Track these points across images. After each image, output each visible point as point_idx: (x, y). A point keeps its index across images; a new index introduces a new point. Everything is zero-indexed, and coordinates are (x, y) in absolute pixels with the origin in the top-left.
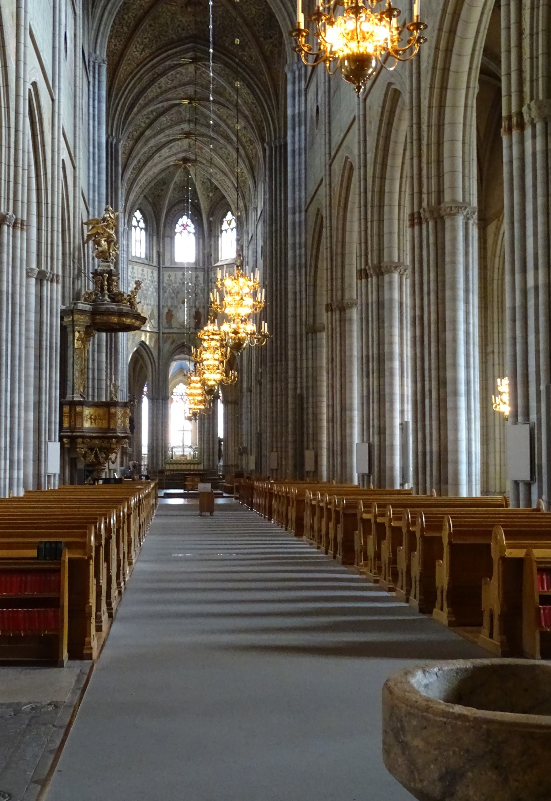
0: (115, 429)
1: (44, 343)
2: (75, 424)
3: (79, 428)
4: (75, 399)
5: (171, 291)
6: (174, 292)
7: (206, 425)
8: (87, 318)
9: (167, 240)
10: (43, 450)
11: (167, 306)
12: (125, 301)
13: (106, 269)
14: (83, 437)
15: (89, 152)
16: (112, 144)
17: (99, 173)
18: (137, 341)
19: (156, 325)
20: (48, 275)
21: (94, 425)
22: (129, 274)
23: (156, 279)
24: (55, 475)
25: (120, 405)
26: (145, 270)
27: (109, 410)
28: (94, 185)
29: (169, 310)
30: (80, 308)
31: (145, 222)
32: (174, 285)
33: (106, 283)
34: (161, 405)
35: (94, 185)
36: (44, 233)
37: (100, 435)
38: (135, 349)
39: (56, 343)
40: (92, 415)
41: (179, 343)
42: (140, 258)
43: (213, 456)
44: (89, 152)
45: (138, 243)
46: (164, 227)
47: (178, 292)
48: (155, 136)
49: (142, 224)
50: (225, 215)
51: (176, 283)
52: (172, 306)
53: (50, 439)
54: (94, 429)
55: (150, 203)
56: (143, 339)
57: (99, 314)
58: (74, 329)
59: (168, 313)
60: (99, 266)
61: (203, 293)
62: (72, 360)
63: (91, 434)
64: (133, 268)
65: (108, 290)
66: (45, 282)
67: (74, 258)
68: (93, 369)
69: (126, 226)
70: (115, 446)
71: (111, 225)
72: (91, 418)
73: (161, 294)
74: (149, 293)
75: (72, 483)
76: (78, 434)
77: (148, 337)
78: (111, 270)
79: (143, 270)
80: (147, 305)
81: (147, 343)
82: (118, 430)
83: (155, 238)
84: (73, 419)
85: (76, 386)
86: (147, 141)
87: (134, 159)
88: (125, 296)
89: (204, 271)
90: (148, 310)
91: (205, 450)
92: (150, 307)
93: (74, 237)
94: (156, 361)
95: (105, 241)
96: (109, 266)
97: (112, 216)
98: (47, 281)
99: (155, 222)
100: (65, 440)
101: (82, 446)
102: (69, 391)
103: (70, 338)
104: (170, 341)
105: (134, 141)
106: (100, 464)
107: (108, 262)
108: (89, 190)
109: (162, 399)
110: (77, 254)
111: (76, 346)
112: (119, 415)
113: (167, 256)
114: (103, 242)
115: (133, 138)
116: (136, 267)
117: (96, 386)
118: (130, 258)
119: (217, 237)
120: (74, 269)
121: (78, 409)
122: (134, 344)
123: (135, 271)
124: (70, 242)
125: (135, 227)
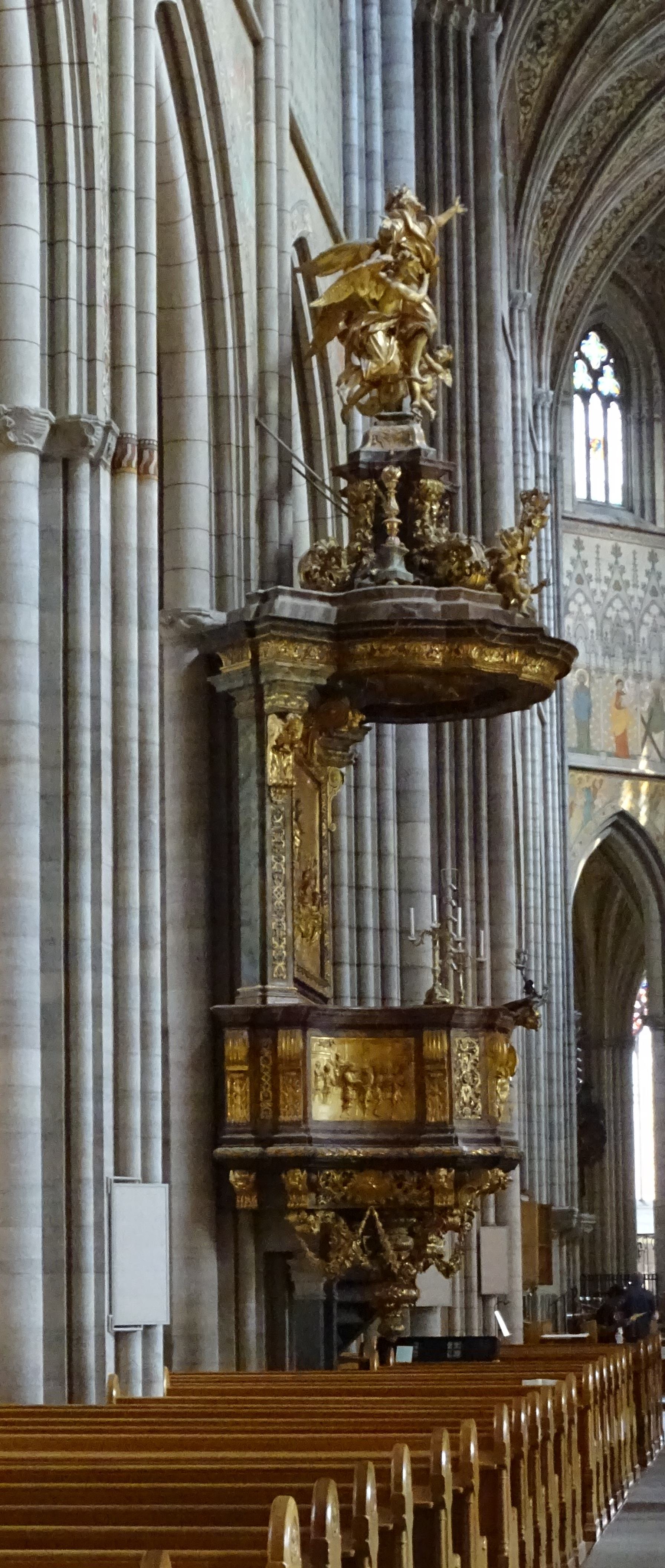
0: (444, 1127)
1: (86, 740)
2: (276, 1111)
3: (296, 1125)
4: (270, 1001)
8: (315, 653)
10: (89, 1218)
12: (477, 578)
13: (393, 447)
14: (309, 1163)
15: (344, 24)
16: (460, 35)
17: (387, 105)
18: (603, 815)
20: (95, 439)
21: (355, 1112)
22: (566, 566)
24: (148, 1329)
25: (468, 1020)
26: (626, 549)
27: (419, 1047)
28: (368, 155)
30: (286, 614)
31: (621, 373)
33: (394, 504)
35: (368, 155)
36: (74, 256)
37: (384, 1151)
38: (598, 841)
39: (143, 743)
40: (347, 1068)
42: (605, 506)
44: (344, 24)
45: (597, 456)
48: (640, 28)
49: (610, 384)
53: (121, 1168)
54: (358, 1126)
55: (639, 304)
56: (626, 804)
57: (365, 636)
58: (260, 700)
60: (366, 439)
62: (255, 833)
63: (345, 1151)
64: (579, 545)
65: (405, 533)
66: (85, 470)
67: (263, 412)
68: (382, 891)
69: (546, 384)
70: (450, 1200)
71: (414, 266)
72: (343, 1081)
74: (644, 633)
75: (274, 1362)
76: (288, 1149)
77: (643, 798)
78: (418, 451)
79: (616, 552)
80: (638, 676)
81: (643, 820)
82: (461, 1130)
84: (266, 1090)
85: (278, 947)
86: (612, 50)
87: (564, 121)
88: (478, 553)
90: (639, 697)
92: (647, 686)
93: (262, 330)
95: (390, 332)
96: (408, 437)
97: (419, 229)
98: (95, 465)
100: (234, 1176)
101: (308, 1201)
102: (248, 969)
103: (247, 742)
105: (559, 55)
106: (388, 1277)
107: (402, 419)
108: (346, 174)
110: (273, 396)
111: (273, 776)
112: (465, 1063)
114: (380, 337)
115: (555, 45)
116: (590, 542)
117: (395, 959)
118: (568, 508)
120: (263, 458)
121: (288, 1043)
122: (591, 825)
123: (588, 554)
124: (241, 347)
125: (585, 395)
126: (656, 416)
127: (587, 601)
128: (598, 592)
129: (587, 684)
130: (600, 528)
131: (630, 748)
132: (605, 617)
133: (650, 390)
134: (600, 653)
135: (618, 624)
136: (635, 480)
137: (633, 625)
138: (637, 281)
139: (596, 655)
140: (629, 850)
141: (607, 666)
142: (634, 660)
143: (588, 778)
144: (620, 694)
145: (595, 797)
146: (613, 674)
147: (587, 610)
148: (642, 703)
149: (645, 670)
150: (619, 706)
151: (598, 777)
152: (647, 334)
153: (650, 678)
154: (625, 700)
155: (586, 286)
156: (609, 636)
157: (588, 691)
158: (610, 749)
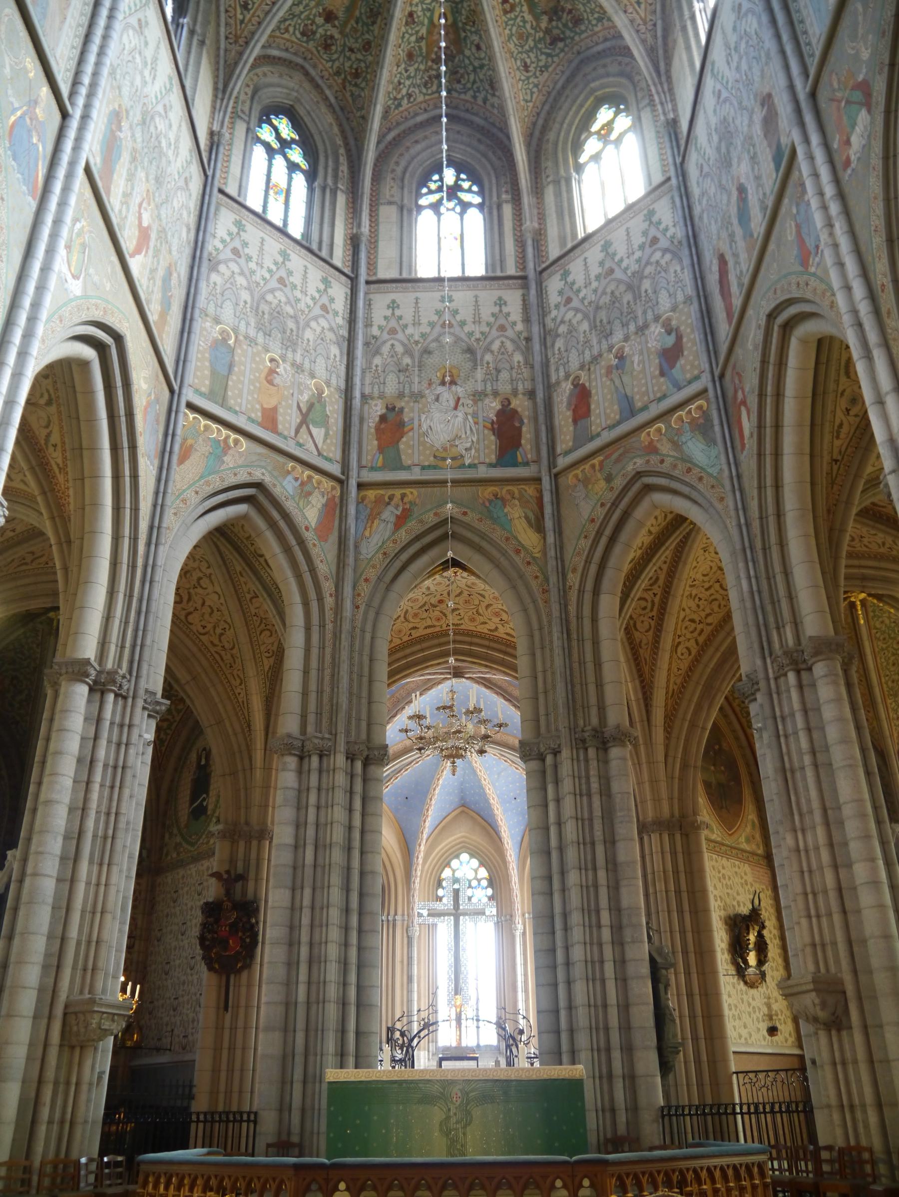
5: (399, 349)
6: (408, 352)
7: (573, 878)
9: (388, 213)
11: (382, 396)
19: (336, 453)
23: (340, 303)
29: (391, 409)
31: (310, 153)
32: (409, 331)
34: (341, 779)
41: (431, 519)
43: (628, 1049)
46: (377, 178)
47: (427, 352)
49: (296, 155)
50: (591, 116)
51: (417, 323)
52: (401, 395)
59: (383, 418)
61: (527, 351)
73: (359, 363)
74: (308, 334)
80: (298, 368)
83: (341, 199)
89: (526, 287)
91: (582, 1017)
94: (328, 587)
99: (343, 160)
104: (389, 514)
109: (351, 757)
113: (387, 252)
119: (563, 185)
126: (340, 186)
127: (242, 273)
128: (258, 274)
129: (231, 342)
130: (268, 228)
131: (280, 427)
132: (263, 297)
133: (336, 170)
134: (253, 324)
135: (277, 313)
136: (315, 227)
137: (297, 322)
138: (330, 87)
139: (248, 324)
140: (269, 535)
141: (260, 340)
142: (294, 351)
143: (219, 430)
144: (272, 372)
145: (225, 454)
146: (268, 351)
147: (241, 281)
148: (301, 393)
149: (307, 365)
150: (270, 382)
151: (233, 436)
152: (336, 130)
153: (312, 376)
154: (278, 380)
155: (267, 8)
156: (266, 316)
157: (232, 351)
158: (253, 415)
